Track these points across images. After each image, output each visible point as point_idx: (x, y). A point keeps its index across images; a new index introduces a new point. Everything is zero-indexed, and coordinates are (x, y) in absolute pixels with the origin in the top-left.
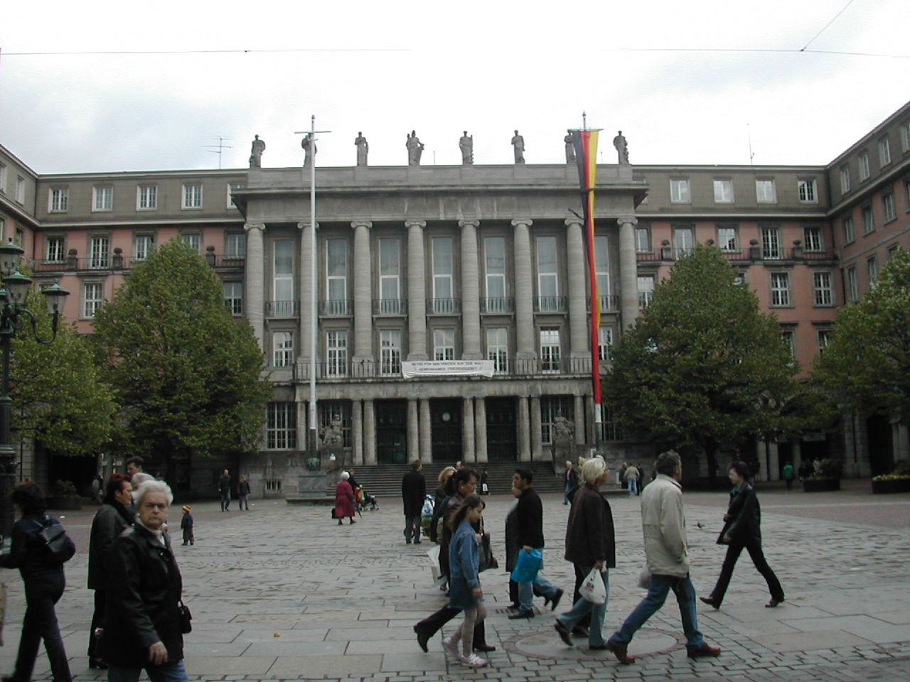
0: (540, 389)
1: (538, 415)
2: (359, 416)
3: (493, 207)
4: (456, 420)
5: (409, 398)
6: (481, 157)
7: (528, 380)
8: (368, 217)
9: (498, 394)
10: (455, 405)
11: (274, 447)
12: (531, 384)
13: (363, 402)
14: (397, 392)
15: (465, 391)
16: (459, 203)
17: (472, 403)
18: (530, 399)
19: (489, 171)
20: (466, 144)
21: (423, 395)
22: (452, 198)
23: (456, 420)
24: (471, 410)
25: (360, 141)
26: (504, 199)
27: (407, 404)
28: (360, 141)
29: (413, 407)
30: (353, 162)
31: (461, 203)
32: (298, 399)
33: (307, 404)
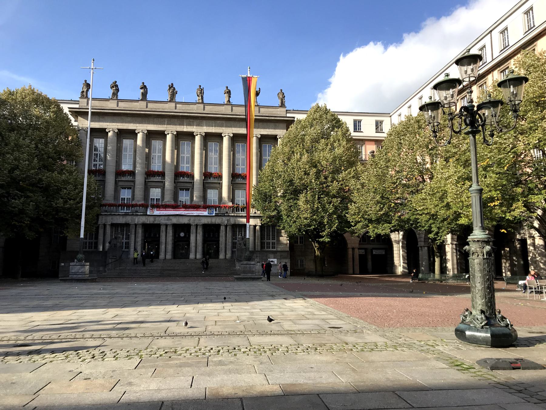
0: (232, 221)
1: (229, 235)
2: (133, 233)
4: (187, 236)
5: (161, 223)
9: (209, 223)
10: (186, 228)
11: (92, 248)
12: (228, 218)
13: (136, 225)
14: (155, 220)
15: (192, 221)
17: (195, 227)
18: (226, 226)
21: (169, 222)
23: (187, 236)
24: (194, 231)
25: (144, 87)
27: (160, 227)
29: (163, 228)
32: (99, 222)
33: (105, 225)
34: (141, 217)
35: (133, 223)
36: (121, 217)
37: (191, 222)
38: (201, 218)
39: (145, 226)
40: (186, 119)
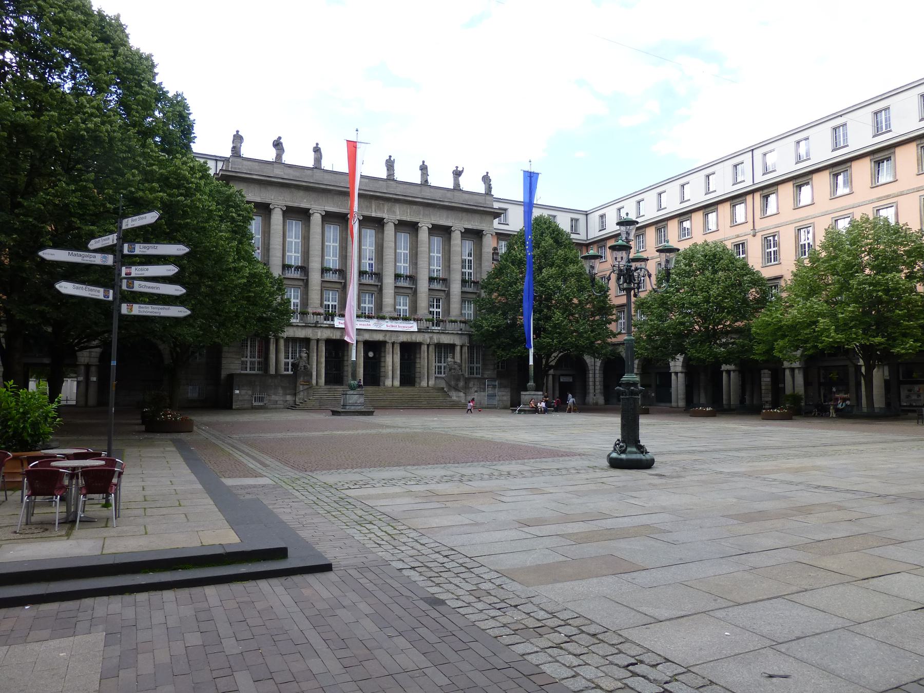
3: (407, 213)
6: (400, 176)
7: (429, 332)
8: (323, 207)
9: (409, 340)
12: (431, 335)
13: (318, 341)
16: (386, 207)
18: (428, 345)
19: (408, 186)
20: (390, 164)
22: (381, 202)
25: (317, 150)
26: (414, 207)
28: (317, 150)
30: (310, 163)
31: (387, 206)
34: (325, 330)
35: (315, 338)
36: (300, 329)
37: (387, 339)
38: (399, 334)
39: (329, 342)
40: (375, 200)
